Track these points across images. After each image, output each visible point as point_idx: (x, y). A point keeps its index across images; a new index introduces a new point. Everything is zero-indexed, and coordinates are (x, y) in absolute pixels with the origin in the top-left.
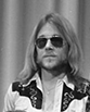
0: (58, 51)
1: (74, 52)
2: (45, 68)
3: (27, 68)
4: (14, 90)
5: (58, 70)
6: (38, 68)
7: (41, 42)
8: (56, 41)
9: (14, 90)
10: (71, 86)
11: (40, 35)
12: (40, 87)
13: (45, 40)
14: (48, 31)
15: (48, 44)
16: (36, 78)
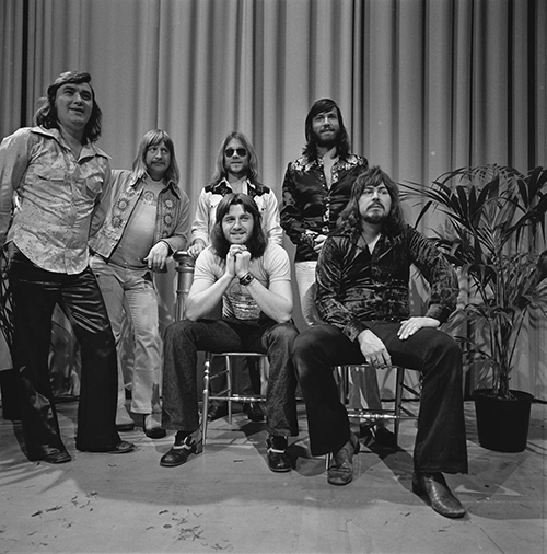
0: (243, 159)
1: (253, 160)
2: (232, 172)
3: (216, 171)
4: (207, 191)
5: (240, 175)
6: (226, 172)
7: (230, 152)
8: (241, 152)
9: (207, 191)
10: (254, 187)
11: (148, 161)
12: (228, 186)
13: (232, 151)
14: (234, 144)
15: (235, 154)
16: (224, 180)
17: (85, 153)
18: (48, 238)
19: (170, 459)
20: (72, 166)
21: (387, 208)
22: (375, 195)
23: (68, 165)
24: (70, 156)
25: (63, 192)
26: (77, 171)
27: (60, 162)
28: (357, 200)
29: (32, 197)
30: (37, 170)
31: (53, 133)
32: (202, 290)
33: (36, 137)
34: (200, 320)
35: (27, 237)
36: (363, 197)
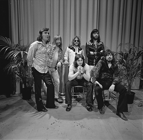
17: (47, 46)
18: (41, 66)
19: (68, 110)
20: (45, 49)
21: (112, 59)
22: (109, 56)
23: (44, 49)
24: (45, 47)
25: (44, 56)
26: (46, 51)
27: (43, 49)
28: (106, 57)
29: (37, 57)
30: (39, 51)
31: (41, 42)
32: (72, 75)
33: (38, 44)
34: (71, 81)
35: (37, 66)
36: (107, 57)
